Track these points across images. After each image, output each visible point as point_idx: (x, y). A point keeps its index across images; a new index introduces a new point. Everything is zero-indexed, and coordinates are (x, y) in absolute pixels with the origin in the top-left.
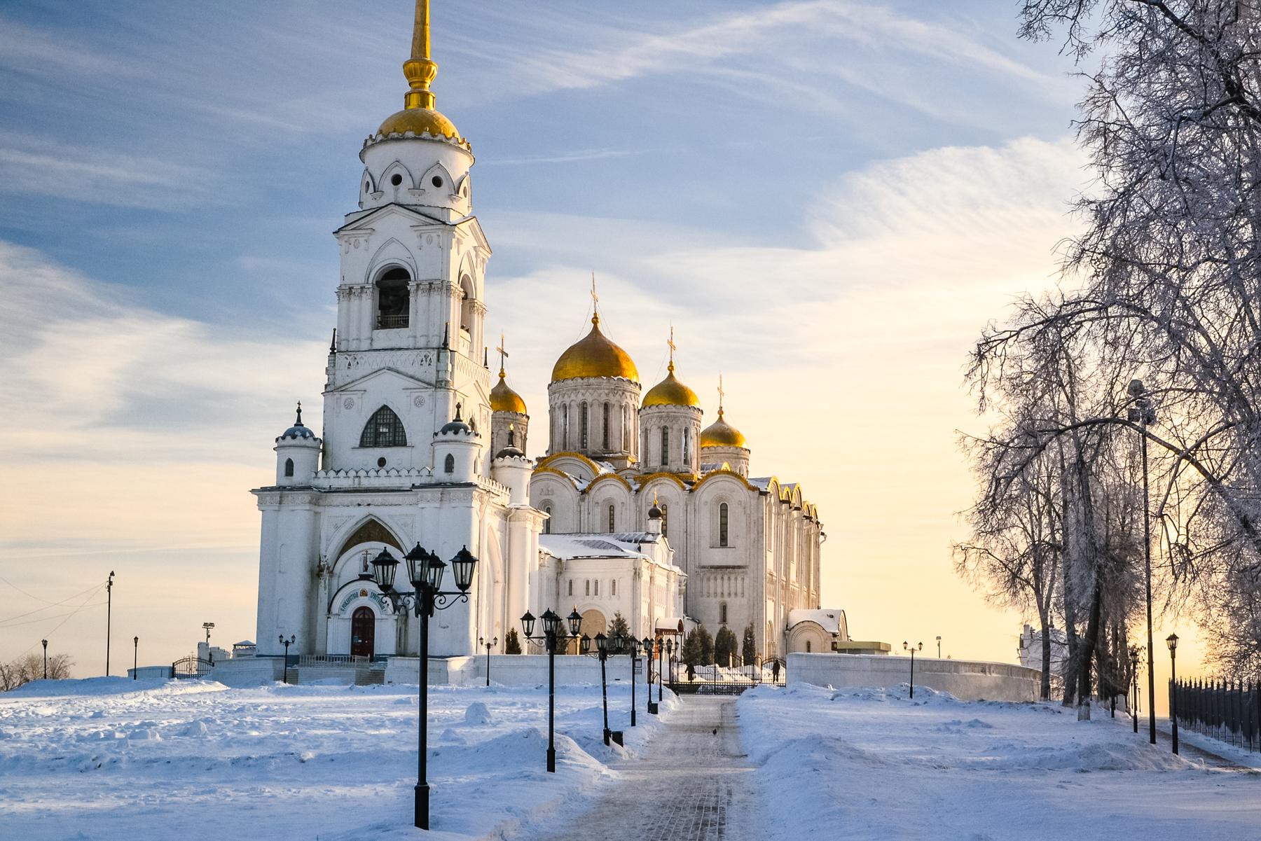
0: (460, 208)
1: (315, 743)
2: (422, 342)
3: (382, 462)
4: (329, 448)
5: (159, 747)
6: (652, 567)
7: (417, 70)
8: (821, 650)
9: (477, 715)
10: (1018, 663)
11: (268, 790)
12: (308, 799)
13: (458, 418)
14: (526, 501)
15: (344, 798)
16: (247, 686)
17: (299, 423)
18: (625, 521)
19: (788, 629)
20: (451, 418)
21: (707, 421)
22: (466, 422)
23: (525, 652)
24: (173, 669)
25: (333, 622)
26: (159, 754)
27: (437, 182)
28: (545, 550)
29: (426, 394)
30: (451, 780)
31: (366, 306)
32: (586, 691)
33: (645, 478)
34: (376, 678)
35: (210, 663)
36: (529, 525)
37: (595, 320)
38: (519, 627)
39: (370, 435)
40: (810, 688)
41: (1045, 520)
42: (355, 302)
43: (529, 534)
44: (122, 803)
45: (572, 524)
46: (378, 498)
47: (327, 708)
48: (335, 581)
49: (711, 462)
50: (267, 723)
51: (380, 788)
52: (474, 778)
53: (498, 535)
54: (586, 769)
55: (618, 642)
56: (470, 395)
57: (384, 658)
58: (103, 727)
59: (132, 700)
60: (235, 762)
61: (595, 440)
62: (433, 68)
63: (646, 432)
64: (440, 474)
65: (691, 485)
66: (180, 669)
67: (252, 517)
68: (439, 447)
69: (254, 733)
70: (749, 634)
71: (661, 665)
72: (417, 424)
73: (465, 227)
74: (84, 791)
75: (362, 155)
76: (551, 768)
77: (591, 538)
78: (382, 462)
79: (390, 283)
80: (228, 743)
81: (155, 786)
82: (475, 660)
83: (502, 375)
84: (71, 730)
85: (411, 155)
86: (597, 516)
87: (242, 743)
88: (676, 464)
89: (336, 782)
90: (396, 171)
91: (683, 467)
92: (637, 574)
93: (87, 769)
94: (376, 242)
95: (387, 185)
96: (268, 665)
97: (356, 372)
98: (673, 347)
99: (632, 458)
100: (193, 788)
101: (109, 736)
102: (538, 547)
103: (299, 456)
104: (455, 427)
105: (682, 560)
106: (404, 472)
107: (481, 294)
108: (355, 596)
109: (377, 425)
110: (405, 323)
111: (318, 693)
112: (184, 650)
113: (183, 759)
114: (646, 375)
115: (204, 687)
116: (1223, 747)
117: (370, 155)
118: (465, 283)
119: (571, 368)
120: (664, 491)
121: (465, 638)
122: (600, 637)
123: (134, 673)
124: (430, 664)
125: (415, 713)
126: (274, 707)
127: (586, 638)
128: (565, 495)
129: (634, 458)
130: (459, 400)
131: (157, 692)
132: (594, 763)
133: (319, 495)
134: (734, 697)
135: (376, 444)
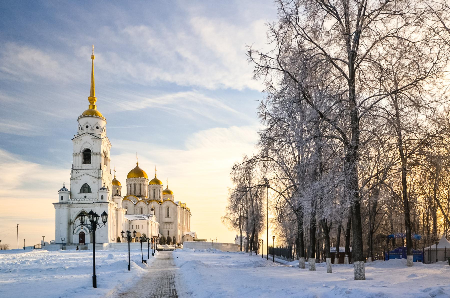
0: (103, 135)
1: (70, 264)
2: (95, 168)
3: (85, 197)
4: (72, 193)
5: (29, 266)
6: (152, 222)
7: (92, 99)
8: (191, 241)
9: (110, 257)
10: (234, 243)
11: (55, 277)
12: (66, 279)
13: (104, 186)
14: (121, 206)
15: (76, 278)
16: (53, 251)
17: (64, 187)
18: (145, 211)
19: (183, 236)
20: (102, 186)
21: (164, 188)
22: (106, 187)
23: (122, 242)
24: (34, 247)
25: (74, 235)
26: (29, 268)
27: (97, 128)
28: (126, 218)
29: (96, 180)
30: (104, 273)
31: (80, 159)
32: (136, 251)
33: (150, 201)
34: (86, 248)
35: (44, 245)
36: (122, 212)
37: (137, 164)
38: (120, 235)
39: (82, 191)
40: (189, 249)
41: (242, 211)
42: (77, 157)
43: (122, 214)
44: (15, 281)
45: (133, 212)
46: (85, 205)
47: (73, 256)
48: (75, 225)
49: (165, 198)
50: (58, 259)
51: (85, 275)
52: (110, 272)
53: (115, 215)
54: (137, 269)
55: (144, 239)
56: (107, 181)
57: (87, 244)
58: (15, 261)
59: (23, 255)
60: (47, 270)
61: (138, 193)
62: (96, 99)
63: (150, 190)
64: (100, 200)
65: (161, 203)
66: (36, 247)
67: (53, 210)
68: (99, 193)
69: (54, 262)
70: (174, 237)
71: (155, 244)
72: (94, 187)
73: (105, 139)
74: (5, 278)
75: (78, 120)
76: (129, 269)
77: (137, 215)
78: (85, 197)
79: (86, 153)
80: (47, 265)
81: (25, 276)
82: (110, 244)
83: (115, 177)
84: (6, 262)
85: (91, 121)
86: (139, 210)
87: (50, 265)
88: (156, 199)
89: (74, 274)
90: (87, 125)
91: (159, 199)
92: (148, 224)
93: (8, 272)
94: (82, 142)
95: (85, 128)
96: (58, 246)
97: (79, 175)
98: (156, 170)
99: (147, 197)
100: (35, 277)
101: (16, 263)
102: (124, 217)
103: (64, 195)
104: (103, 188)
105: (159, 221)
106: (91, 199)
107: (109, 156)
108: (80, 229)
109: (84, 188)
110: (90, 163)
111: (71, 252)
112: (37, 242)
113: (34, 269)
114: (150, 177)
115: (42, 251)
116: (281, 261)
117: (80, 120)
118: (105, 153)
119: (132, 175)
120: (154, 204)
121: (107, 239)
122: (140, 237)
123: (24, 248)
124: (96, 245)
125: (92, 257)
126: (61, 256)
127: (137, 238)
128: (131, 205)
129: (147, 197)
130: (104, 182)
131: (30, 252)
132: (140, 268)
133: (70, 205)
134: (171, 252)
135: (84, 192)
